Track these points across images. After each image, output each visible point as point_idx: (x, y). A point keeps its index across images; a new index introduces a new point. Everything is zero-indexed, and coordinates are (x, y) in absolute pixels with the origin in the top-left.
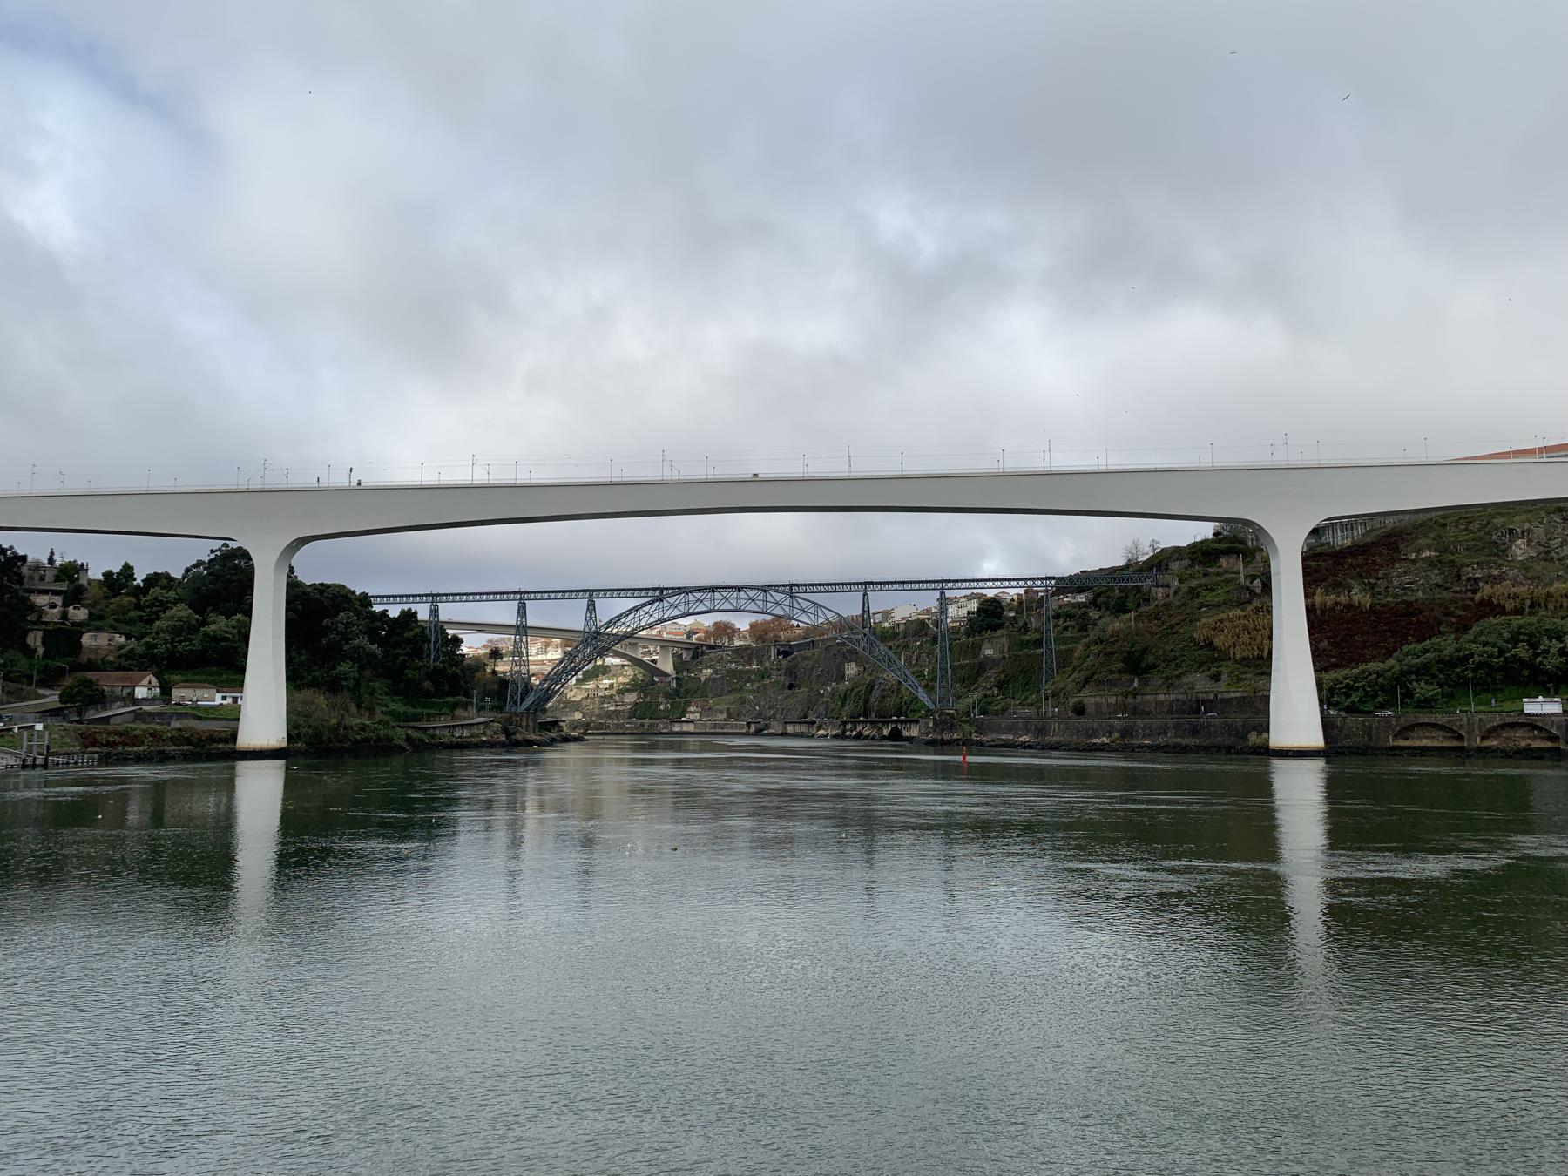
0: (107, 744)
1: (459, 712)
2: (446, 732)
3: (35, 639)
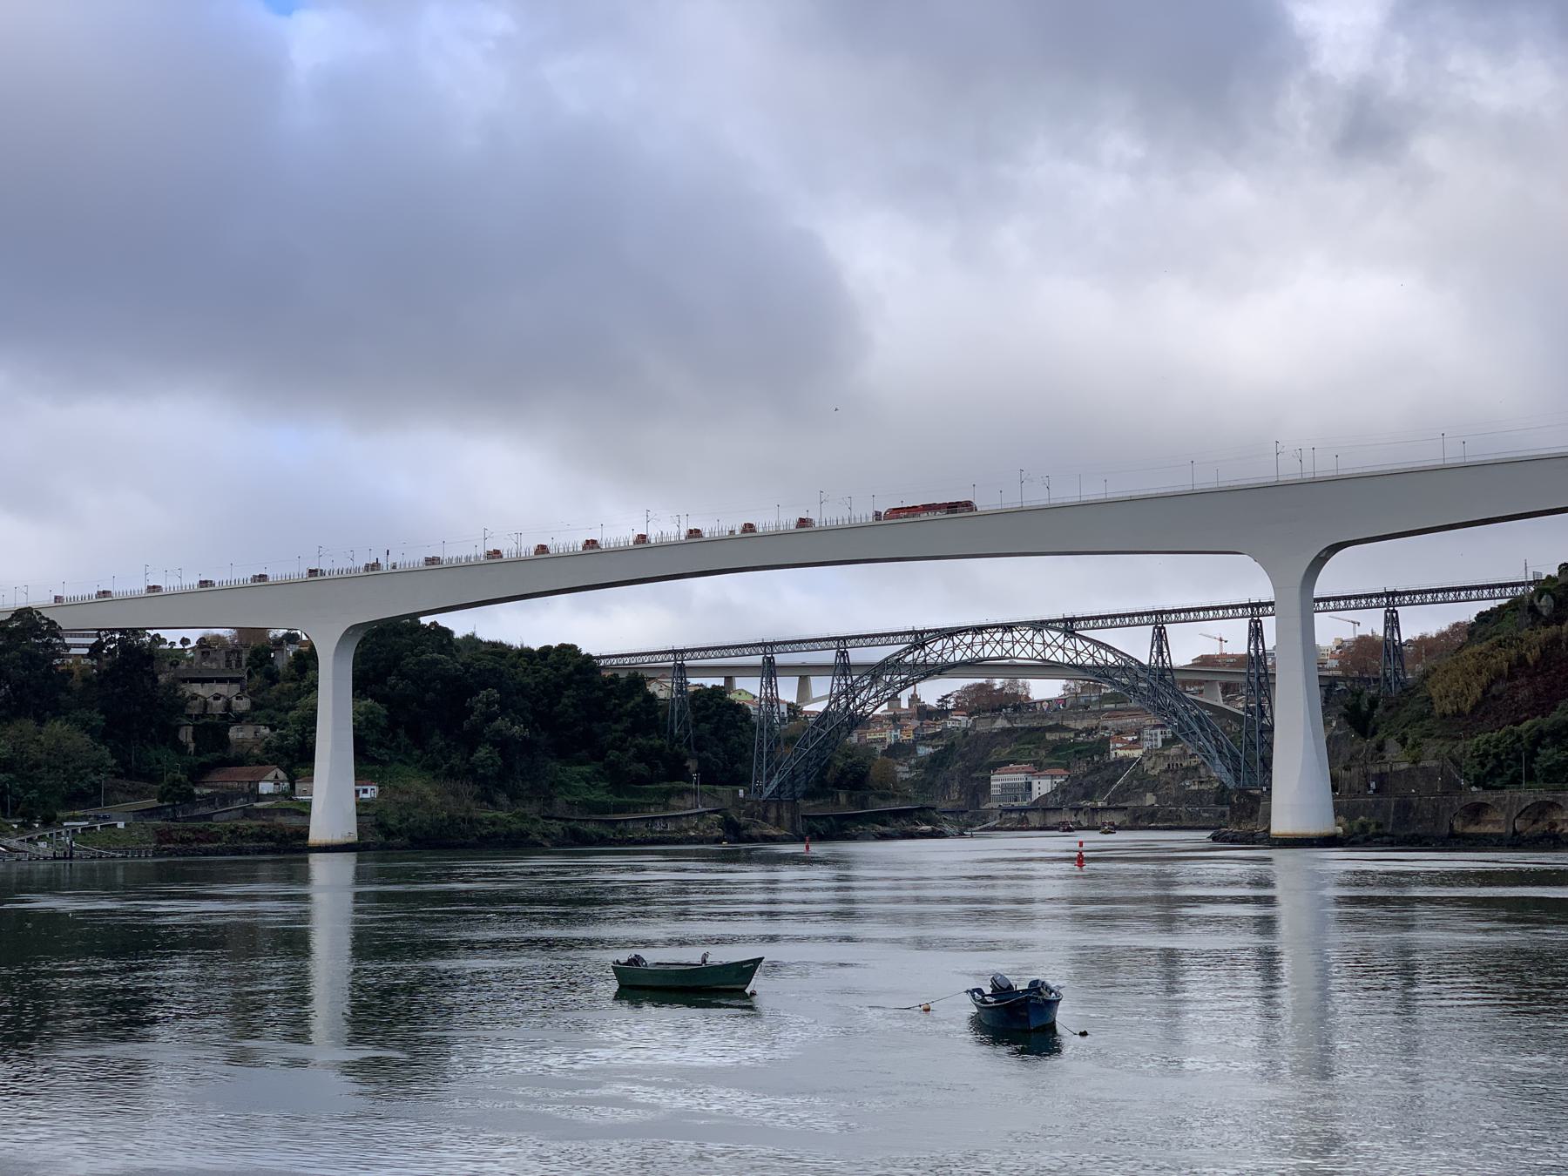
0: (183, 841)
1: (674, 801)
2: (642, 825)
3: (186, 735)
